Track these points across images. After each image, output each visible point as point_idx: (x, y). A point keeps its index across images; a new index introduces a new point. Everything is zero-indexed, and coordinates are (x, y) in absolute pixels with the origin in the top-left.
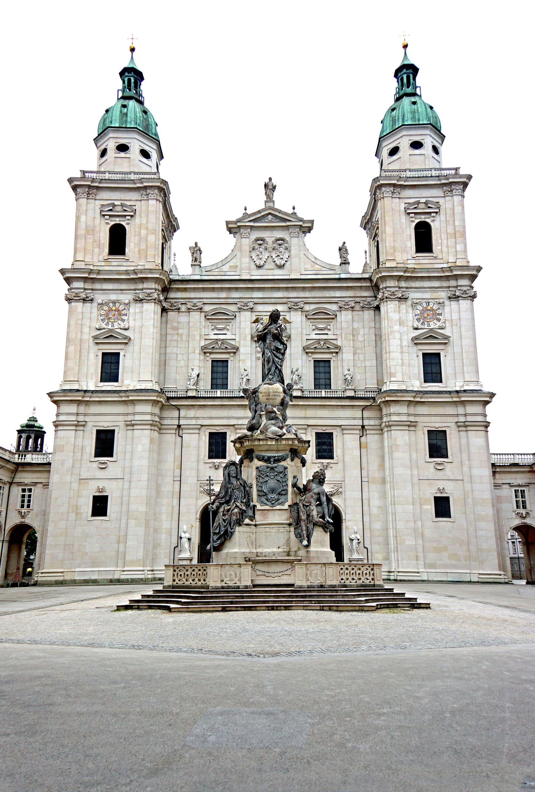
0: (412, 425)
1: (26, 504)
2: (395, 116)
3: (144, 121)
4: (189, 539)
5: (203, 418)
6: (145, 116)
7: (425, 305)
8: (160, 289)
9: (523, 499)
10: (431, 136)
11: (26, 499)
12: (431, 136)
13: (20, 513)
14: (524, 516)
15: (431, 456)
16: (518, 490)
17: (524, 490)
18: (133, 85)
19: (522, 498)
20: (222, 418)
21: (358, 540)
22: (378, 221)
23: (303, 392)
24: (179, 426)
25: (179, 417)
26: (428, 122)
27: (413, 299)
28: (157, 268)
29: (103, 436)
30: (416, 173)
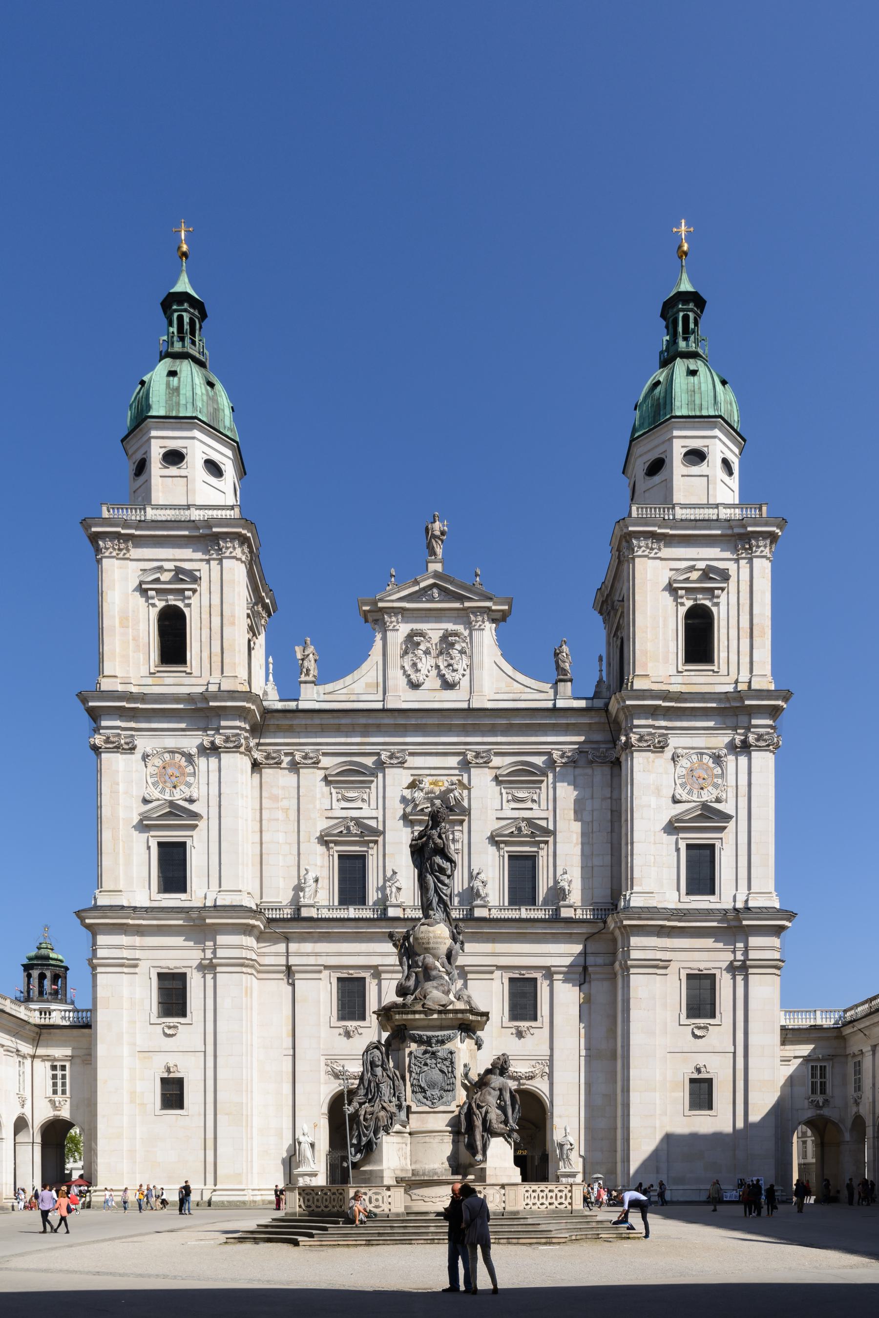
0: (661, 965)
1: (59, 1089)
2: (659, 399)
3: (210, 402)
4: (312, 1145)
5: (328, 954)
6: (211, 393)
7: (694, 757)
8: (248, 728)
9: (823, 1080)
10: (720, 440)
11: (59, 1082)
12: (720, 440)
13: (52, 1102)
14: (821, 1104)
15: (689, 1016)
16: (816, 1066)
17: (825, 1067)
18: (186, 327)
19: (821, 1078)
20: (358, 954)
21: (571, 1145)
22: (623, 601)
23: (490, 910)
24: (289, 968)
25: (287, 952)
26: (717, 414)
27: (675, 748)
28: (241, 688)
29: (168, 984)
30: (692, 511)
